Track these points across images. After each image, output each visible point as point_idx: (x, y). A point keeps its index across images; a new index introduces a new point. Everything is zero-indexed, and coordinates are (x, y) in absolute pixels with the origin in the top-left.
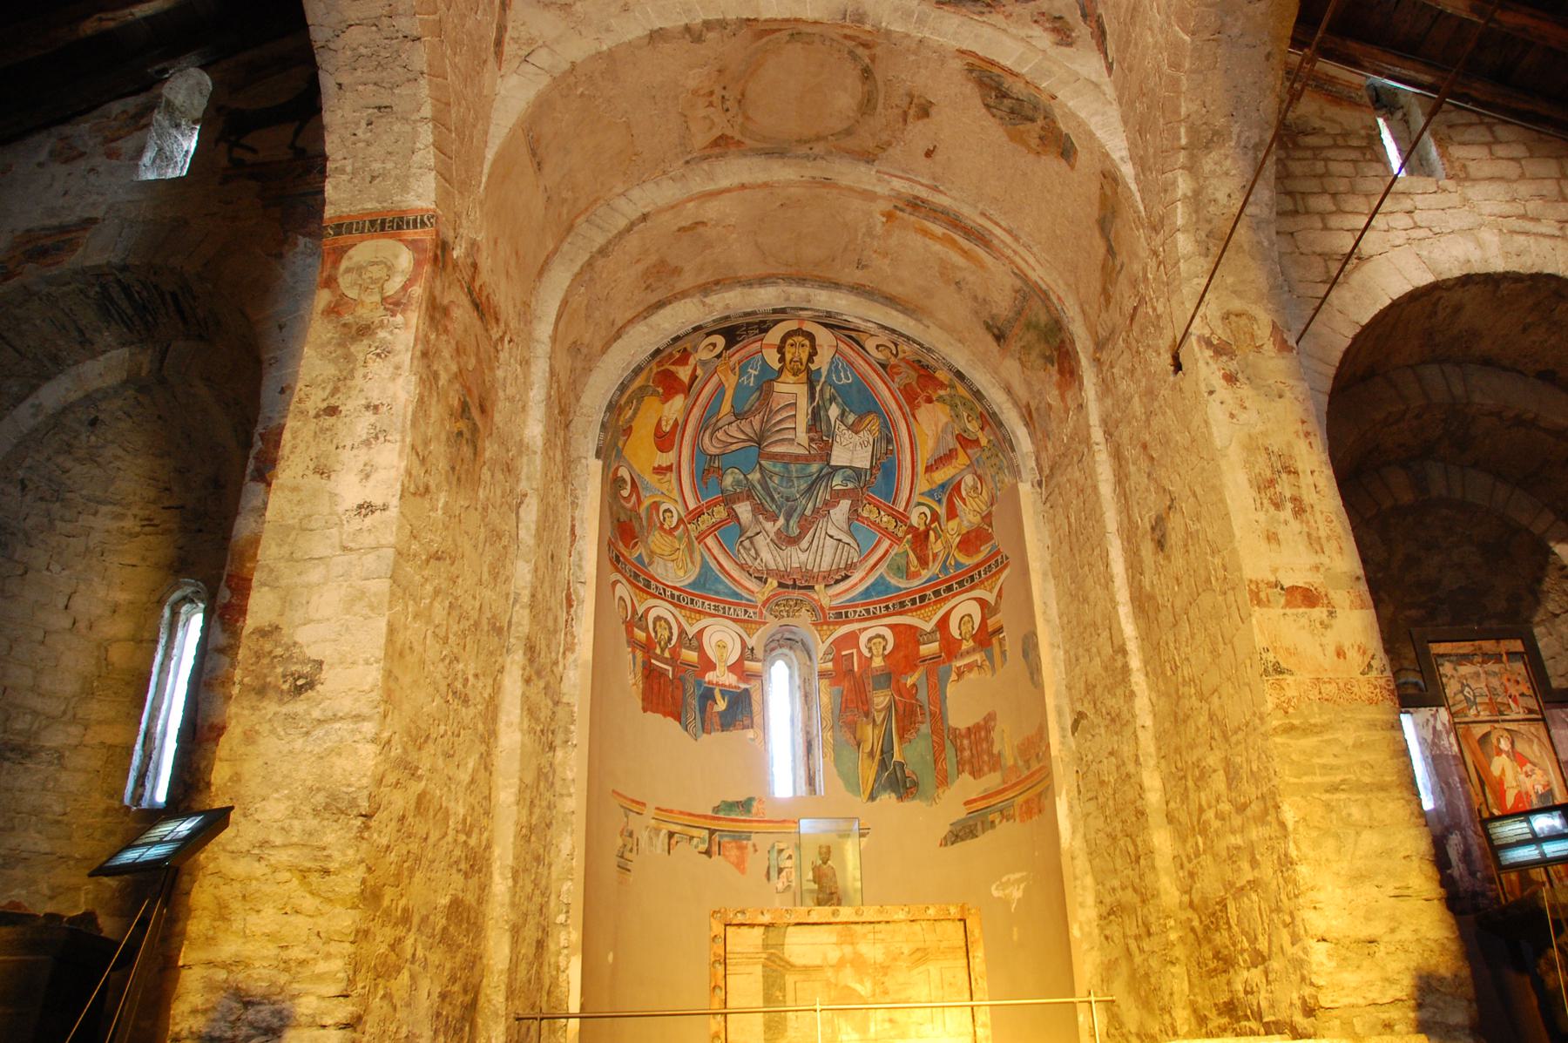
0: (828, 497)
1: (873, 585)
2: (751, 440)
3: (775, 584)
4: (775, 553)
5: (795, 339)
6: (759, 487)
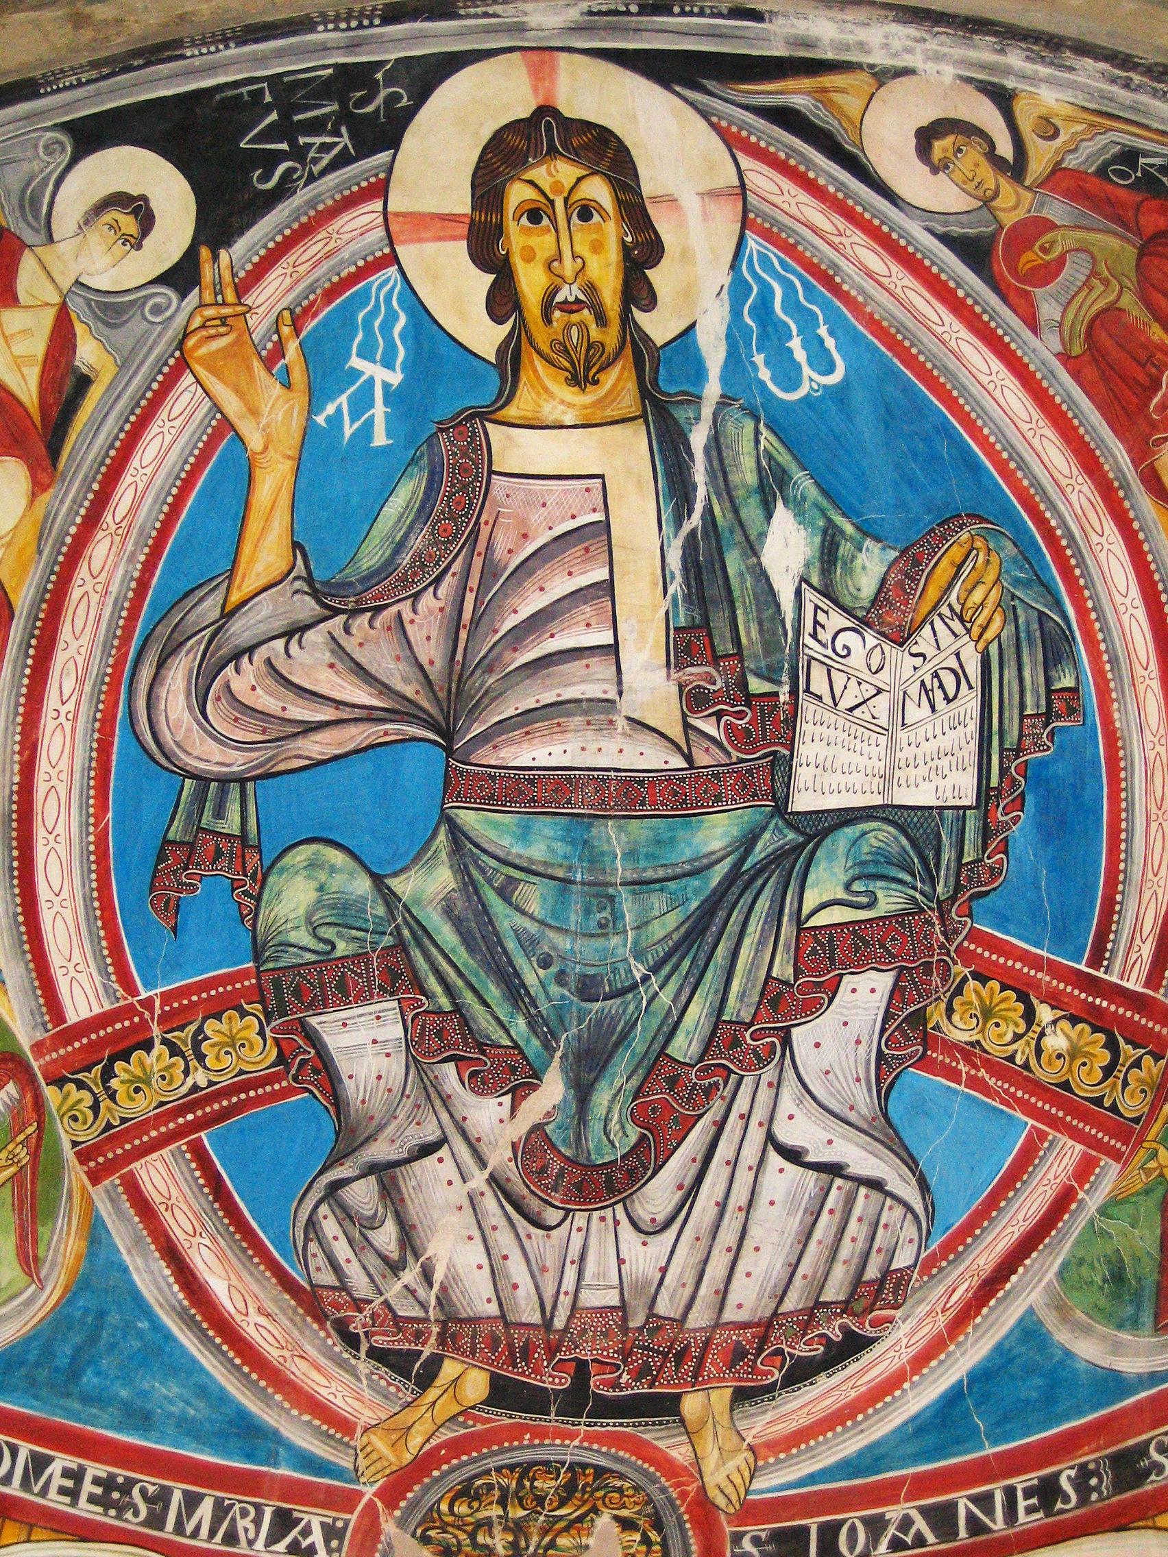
0: (783, 969)
1: (981, 1377)
2: (403, 711)
3: (476, 1385)
4: (504, 1240)
5: (540, 174)
6: (447, 935)
